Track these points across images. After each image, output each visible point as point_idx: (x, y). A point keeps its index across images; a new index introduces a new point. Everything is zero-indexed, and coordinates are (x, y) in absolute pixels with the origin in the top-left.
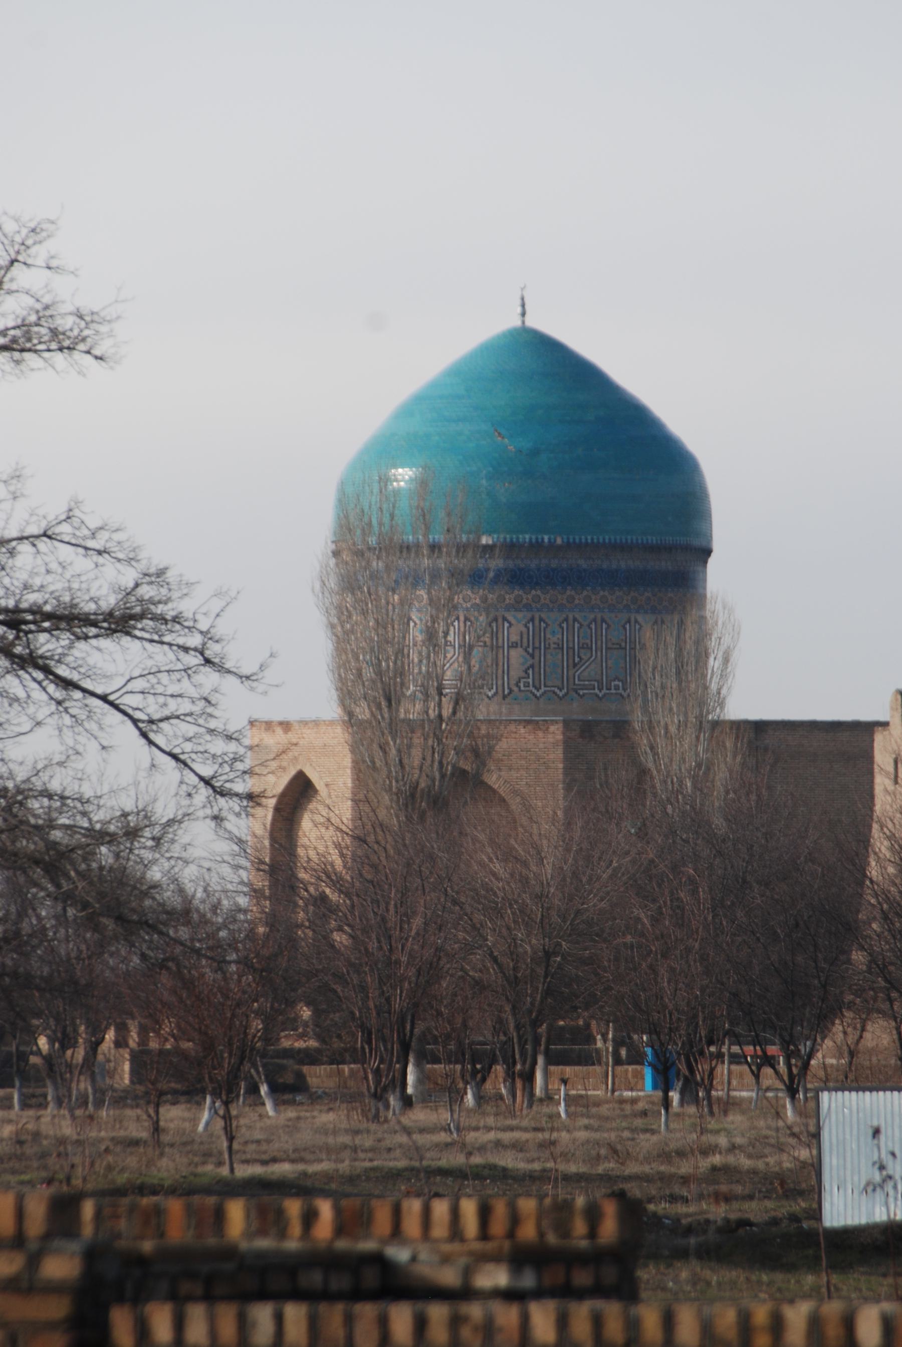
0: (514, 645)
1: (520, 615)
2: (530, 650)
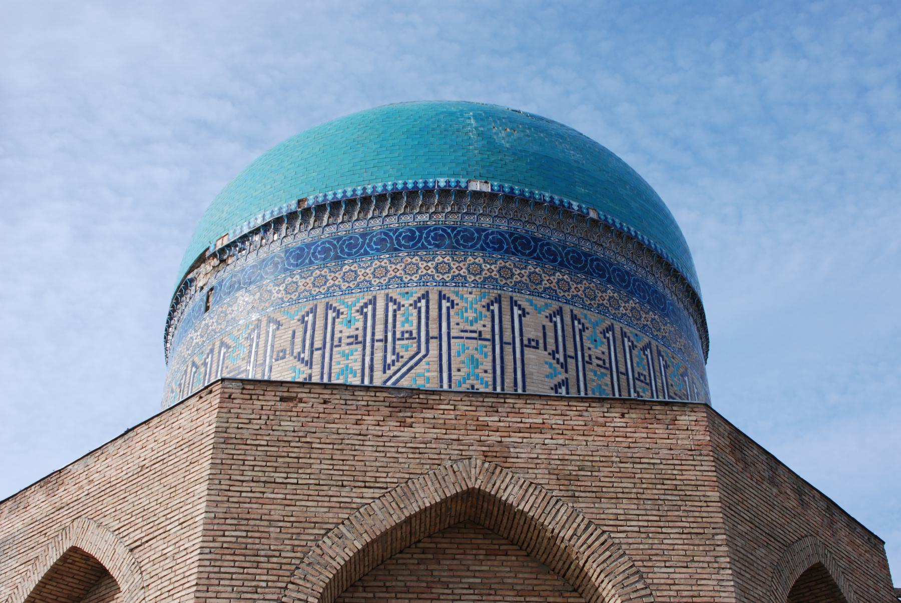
1: (540, 302)
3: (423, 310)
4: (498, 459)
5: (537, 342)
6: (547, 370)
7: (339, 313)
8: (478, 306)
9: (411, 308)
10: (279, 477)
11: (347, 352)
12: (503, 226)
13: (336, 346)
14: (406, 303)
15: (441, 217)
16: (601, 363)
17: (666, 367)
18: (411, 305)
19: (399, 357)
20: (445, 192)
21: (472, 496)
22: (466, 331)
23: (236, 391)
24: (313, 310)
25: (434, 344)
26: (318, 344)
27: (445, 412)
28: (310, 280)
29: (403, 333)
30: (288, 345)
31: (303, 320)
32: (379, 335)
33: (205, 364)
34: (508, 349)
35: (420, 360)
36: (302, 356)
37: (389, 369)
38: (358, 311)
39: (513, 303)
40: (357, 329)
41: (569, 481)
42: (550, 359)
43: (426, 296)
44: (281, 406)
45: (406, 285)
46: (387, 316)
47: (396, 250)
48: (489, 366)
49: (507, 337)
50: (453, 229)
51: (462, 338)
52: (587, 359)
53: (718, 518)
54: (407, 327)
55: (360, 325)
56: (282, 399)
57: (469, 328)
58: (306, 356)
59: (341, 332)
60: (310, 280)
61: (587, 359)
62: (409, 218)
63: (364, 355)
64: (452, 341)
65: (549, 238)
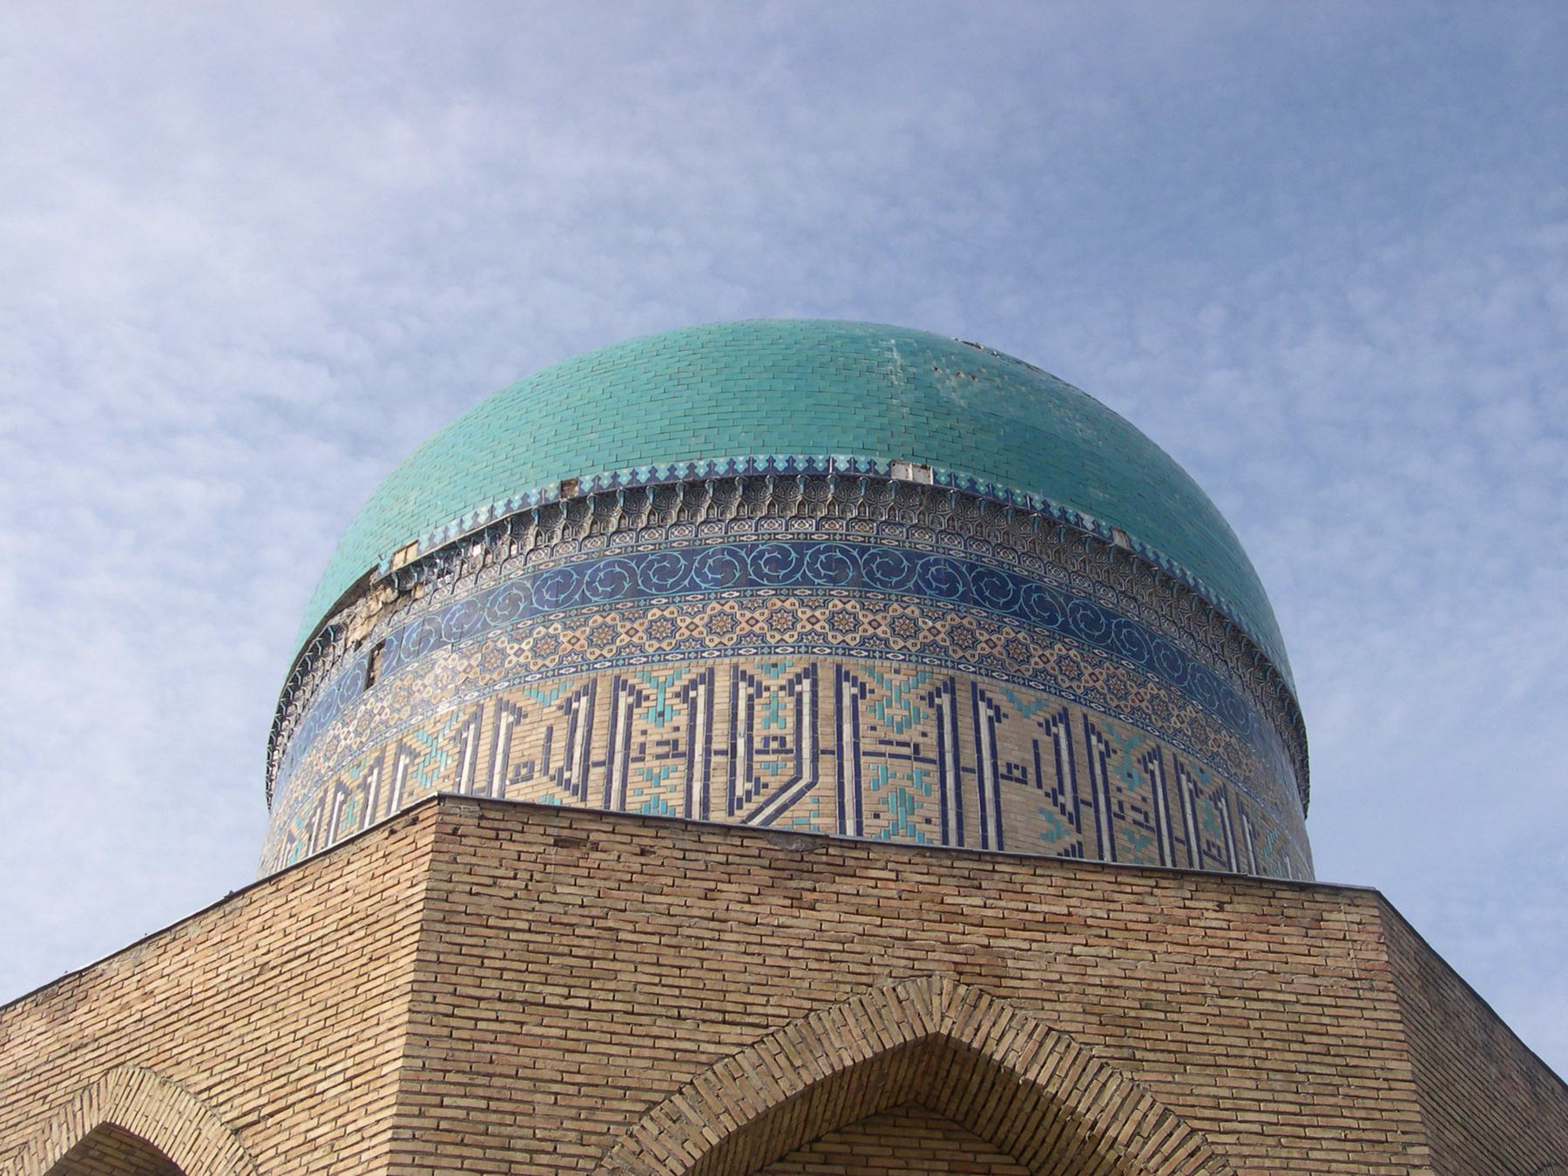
0: (1010, 774)
1: (1027, 696)
2: (1067, 800)
3: (806, 698)
4: (983, 978)
5: (1024, 771)
6: (1041, 822)
7: (640, 698)
8: (912, 697)
9: (782, 693)
10: (553, 994)
11: (656, 771)
12: (957, 550)
13: (635, 760)
14: (774, 684)
15: (839, 527)
16: (1140, 818)
17: (1254, 835)
18: (782, 688)
19: (759, 786)
20: (847, 481)
21: (934, 1053)
22: (890, 743)
23: (466, 819)
24: (590, 691)
25: (827, 764)
26: (598, 754)
27: (877, 885)
28: (582, 634)
29: (766, 740)
30: (537, 755)
31: (567, 708)
32: (720, 743)
33: (365, 787)
34: (970, 780)
35: (801, 793)
36: (567, 775)
37: (740, 807)
38: (677, 695)
39: (978, 695)
40: (677, 729)
41: (1123, 1028)
42: (1047, 804)
43: (811, 672)
44: (556, 855)
45: (772, 650)
46: (735, 707)
47: (752, 583)
48: (934, 812)
49: (969, 759)
50: (863, 551)
51: (883, 755)
52: (1115, 808)
53: (1412, 1113)
54: (775, 730)
55: (682, 720)
56: (559, 842)
57: (895, 737)
58: (575, 775)
59: (644, 733)
60: (582, 634)
61: (1115, 808)
62: (777, 526)
63: (690, 779)
64: (863, 759)
65: (1041, 578)
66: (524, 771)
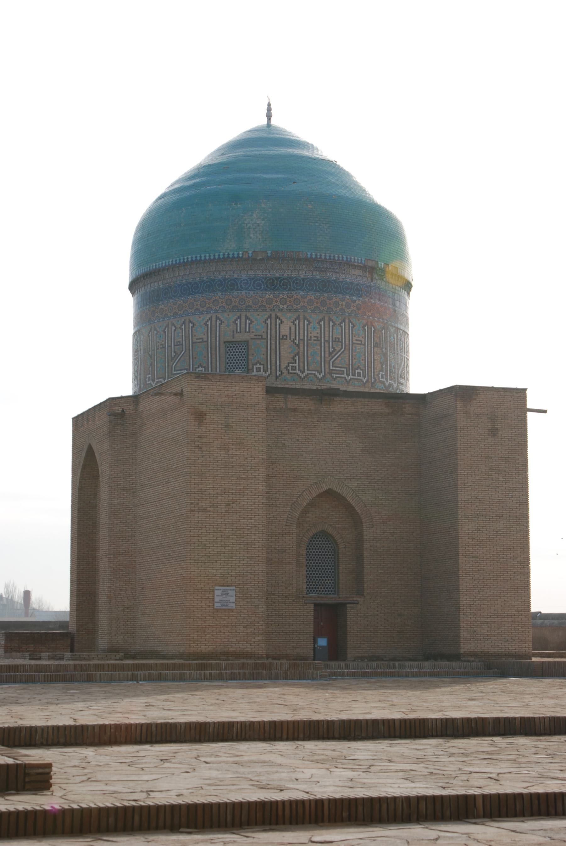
19: (335, 350)
24: (298, 318)
30: (288, 334)
31: (293, 322)
55: (319, 331)
66: (285, 337)
